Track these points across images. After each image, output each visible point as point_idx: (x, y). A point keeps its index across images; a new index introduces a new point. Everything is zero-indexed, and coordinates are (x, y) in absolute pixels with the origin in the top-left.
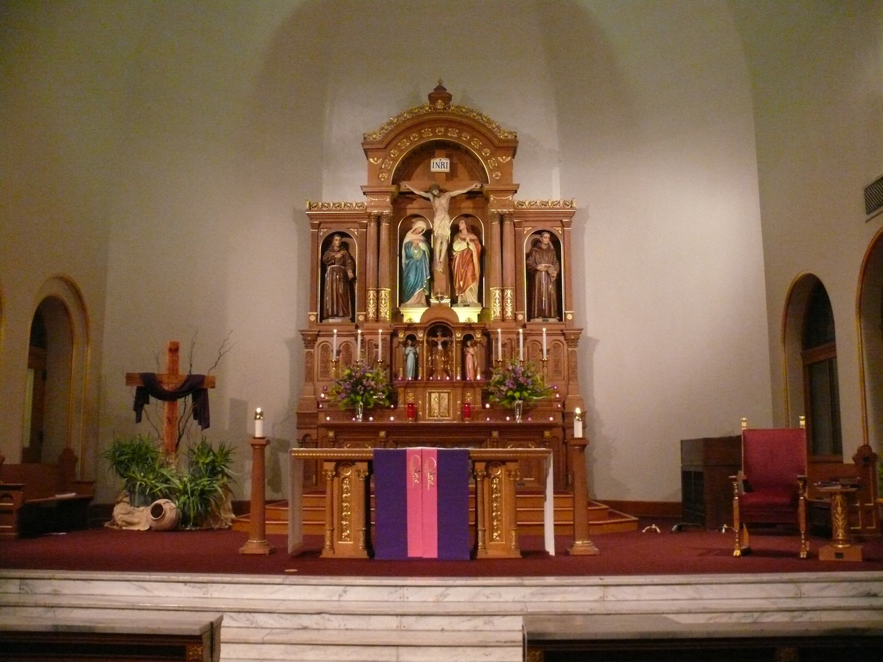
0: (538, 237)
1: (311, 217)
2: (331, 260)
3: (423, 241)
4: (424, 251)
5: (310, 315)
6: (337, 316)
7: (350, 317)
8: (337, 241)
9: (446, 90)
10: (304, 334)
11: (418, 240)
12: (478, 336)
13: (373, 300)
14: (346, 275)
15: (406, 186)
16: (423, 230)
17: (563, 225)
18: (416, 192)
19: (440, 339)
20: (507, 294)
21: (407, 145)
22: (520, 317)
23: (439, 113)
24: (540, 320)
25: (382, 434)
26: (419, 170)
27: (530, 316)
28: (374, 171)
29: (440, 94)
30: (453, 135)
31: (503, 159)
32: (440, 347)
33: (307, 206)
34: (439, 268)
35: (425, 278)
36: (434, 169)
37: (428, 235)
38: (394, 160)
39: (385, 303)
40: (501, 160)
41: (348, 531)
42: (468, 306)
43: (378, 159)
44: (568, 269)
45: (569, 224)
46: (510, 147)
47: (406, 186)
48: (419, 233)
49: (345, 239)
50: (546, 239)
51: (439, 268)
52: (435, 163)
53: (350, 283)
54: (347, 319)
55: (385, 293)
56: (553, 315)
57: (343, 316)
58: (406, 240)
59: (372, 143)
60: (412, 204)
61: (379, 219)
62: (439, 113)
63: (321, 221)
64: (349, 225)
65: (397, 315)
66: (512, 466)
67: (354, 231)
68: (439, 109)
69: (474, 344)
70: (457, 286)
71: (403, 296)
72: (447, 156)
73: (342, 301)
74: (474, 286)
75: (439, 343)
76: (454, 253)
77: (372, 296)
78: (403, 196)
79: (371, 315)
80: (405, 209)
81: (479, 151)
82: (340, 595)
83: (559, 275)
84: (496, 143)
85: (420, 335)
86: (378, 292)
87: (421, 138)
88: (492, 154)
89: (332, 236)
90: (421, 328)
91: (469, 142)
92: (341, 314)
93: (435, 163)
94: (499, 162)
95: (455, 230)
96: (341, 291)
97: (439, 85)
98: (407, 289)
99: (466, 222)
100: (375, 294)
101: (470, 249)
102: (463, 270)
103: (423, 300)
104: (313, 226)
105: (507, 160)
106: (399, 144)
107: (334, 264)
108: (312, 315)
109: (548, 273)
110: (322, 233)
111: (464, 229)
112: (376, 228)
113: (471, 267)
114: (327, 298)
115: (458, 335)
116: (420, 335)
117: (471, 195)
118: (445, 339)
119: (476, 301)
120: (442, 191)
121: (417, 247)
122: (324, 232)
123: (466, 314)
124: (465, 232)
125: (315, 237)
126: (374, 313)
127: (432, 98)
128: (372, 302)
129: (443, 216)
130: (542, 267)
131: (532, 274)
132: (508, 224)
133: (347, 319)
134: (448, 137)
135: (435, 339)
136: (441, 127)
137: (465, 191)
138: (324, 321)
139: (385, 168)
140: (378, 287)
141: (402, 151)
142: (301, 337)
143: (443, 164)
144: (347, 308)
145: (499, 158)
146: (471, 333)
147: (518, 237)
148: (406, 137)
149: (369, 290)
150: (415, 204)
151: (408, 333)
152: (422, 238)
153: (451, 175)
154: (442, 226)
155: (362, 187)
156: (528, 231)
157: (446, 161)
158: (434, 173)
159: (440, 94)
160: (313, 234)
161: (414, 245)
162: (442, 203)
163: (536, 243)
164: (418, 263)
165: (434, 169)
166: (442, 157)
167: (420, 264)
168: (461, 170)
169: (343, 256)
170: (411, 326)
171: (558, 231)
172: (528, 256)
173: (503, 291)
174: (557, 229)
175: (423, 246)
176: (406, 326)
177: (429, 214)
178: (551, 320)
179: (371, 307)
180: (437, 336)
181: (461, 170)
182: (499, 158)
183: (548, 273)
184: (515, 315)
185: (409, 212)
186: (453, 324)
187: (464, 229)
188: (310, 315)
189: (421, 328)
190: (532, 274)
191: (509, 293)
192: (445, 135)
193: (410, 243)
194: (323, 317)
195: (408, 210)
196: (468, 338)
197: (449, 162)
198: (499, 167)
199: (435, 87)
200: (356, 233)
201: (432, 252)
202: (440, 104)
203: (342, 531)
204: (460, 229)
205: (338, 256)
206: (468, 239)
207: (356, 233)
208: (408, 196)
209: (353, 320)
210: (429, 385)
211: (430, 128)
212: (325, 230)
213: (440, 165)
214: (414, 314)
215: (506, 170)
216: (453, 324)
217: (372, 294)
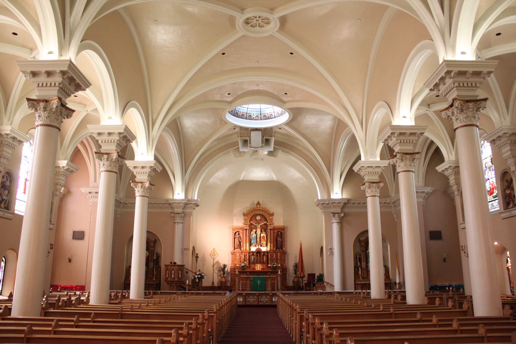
0: (278, 233)
1: (232, 228)
8: (237, 233)
10: (231, 253)
12: (266, 254)
14: (239, 241)
17: (283, 230)
18: (254, 224)
19: (259, 254)
21: (252, 215)
22: (274, 249)
24: (278, 250)
25: (248, 273)
27: (276, 249)
28: (245, 220)
29: (258, 203)
32: (259, 256)
34: (258, 240)
36: (257, 219)
37: (256, 232)
44: (284, 239)
45: (284, 230)
46: (272, 215)
47: (251, 222)
49: (239, 233)
50: (279, 233)
51: (258, 240)
53: (240, 242)
54: (240, 249)
55: (248, 244)
58: (251, 233)
59: (245, 214)
61: (246, 230)
65: (250, 249)
66: (271, 279)
67: (241, 231)
69: (265, 255)
70: (261, 243)
71: (250, 245)
72: (260, 216)
74: (265, 243)
79: (245, 249)
81: (266, 215)
84: (270, 214)
85: (255, 254)
86: (246, 244)
87: (255, 213)
88: (269, 217)
91: (264, 214)
95: (261, 231)
103: (255, 246)
104: (233, 230)
109: (280, 241)
114: (236, 245)
115: (262, 254)
116: (255, 254)
117: (265, 224)
119: (265, 246)
121: (254, 235)
122: (235, 231)
123: (264, 249)
124: (263, 232)
125: (233, 232)
127: (257, 205)
130: (279, 239)
131: (277, 240)
132: (272, 230)
137: (263, 224)
147: (274, 233)
148: (252, 213)
150: (253, 226)
153: (260, 220)
154: (259, 232)
156: (276, 231)
157: (260, 217)
159: (258, 203)
162: (259, 226)
163: (278, 234)
165: (257, 219)
169: (239, 237)
170: (253, 252)
171: (282, 231)
172: (276, 236)
173: (271, 244)
175: (255, 235)
177: (256, 228)
183: (280, 241)
184: (273, 249)
185: (252, 227)
190: (277, 240)
191: (272, 245)
193: (252, 234)
194: (234, 249)
196: (264, 254)
198: (270, 219)
201: (257, 235)
202: (258, 206)
205: (238, 236)
206: (264, 233)
209: (241, 250)
210: (257, 263)
213: (258, 218)
214: (253, 249)
215: (271, 220)
217: (245, 245)
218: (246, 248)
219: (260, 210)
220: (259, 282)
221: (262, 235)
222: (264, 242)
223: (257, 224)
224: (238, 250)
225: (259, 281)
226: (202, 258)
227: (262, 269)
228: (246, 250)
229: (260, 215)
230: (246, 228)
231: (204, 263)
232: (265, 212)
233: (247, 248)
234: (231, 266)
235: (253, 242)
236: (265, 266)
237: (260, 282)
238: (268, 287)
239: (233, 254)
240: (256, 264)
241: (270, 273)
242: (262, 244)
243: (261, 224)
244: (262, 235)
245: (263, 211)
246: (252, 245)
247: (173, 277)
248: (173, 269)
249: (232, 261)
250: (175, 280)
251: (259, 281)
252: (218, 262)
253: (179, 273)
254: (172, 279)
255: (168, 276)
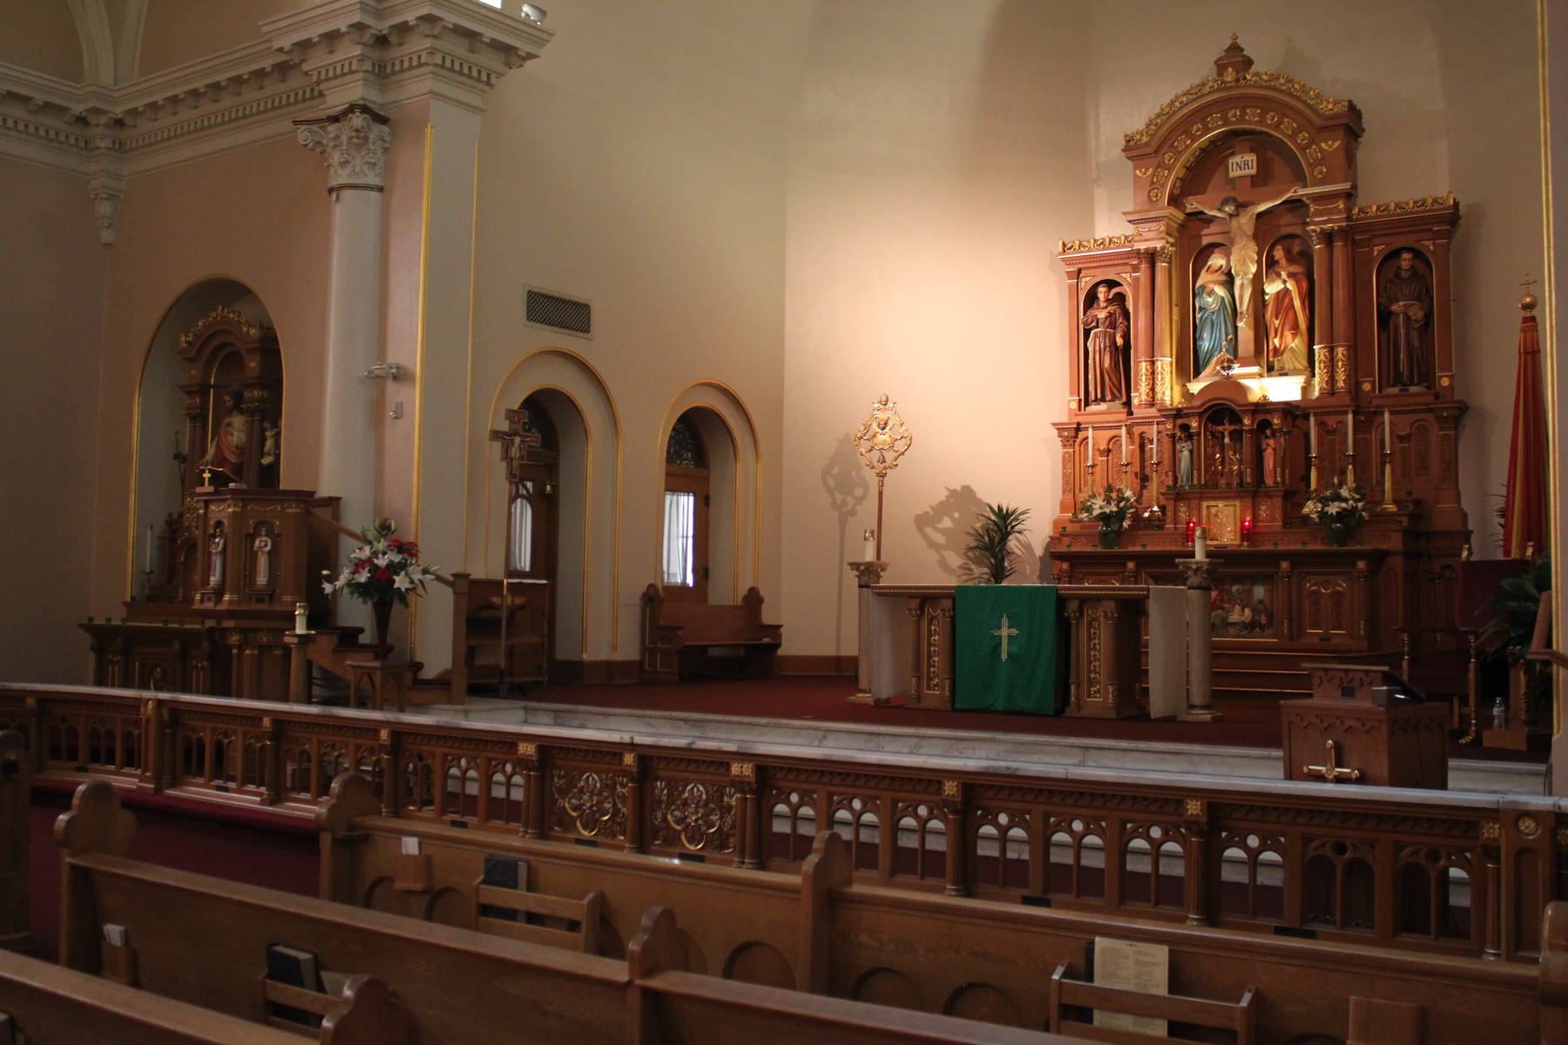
1: (1068, 262)
2: (1092, 322)
3: (1222, 284)
4: (1223, 298)
5: (1070, 401)
6: (1103, 399)
7: (1124, 399)
9: (1242, 50)
10: (1060, 428)
11: (1210, 282)
13: (1146, 375)
15: (1193, 205)
16: (1221, 266)
20: (1337, 354)
22: (1367, 387)
23: (1230, 88)
24: (1394, 390)
26: (1217, 178)
29: (1236, 58)
30: (1252, 119)
31: (1327, 145)
33: (1060, 249)
35: (1224, 338)
36: (1234, 173)
38: (1170, 169)
39: (1162, 379)
40: (1326, 148)
41: (937, 680)
42: (1286, 374)
43: (1147, 170)
47: (1193, 205)
48: (1217, 271)
52: (1235, 166)
54: (1117, 405)
56: (1416, 380)
57: (1111, 401)
59: (1137, 148)
60: (1208, 227)
61: (1151, 257)
62: (1230, 88)
63: (1080, 266)
64: (1119, 269)
67: (1126, 277)
68: (1230, 82)
72: (1252, 151)
73: (1110, 379)
75: (1226, 433)
76: (1267, 297)
77: (1144, 370)
78: (1194, 218)
80: (1200, 237)
82: (820, 741)
83: (1428, 316)
86: (1153, 363)
88: (1312, 142)
89: (1097, 285)
90: (1193, 414)
91: (1277, 126)
92: (1109, 397)
93: (1235, 166)
94: (1321, 150)
96: (1107, 364)
97: (1232, 44)
98: (1201, 356)
99: (1283, 249)
100: (1149, 367)
101: (1288, 289)
102: (1277, 322)
104: (1070, 275)
105: (1335, 147)
106: (1176, 144)
107: (1097, 327)
108: (1073, 400)
109: (1408, 318)
110: (1083, 284)
111: (1281, 259)
112: (1148, 271)
113: (1291, 315)
116: (1194, 424)
118: (1232, 428)
120: (1241, 206)
122: (1086, 282)
126: (1147, 394)
127: (1221, 67)
128: (1144, 378)
129: (1244, 243)
132: (1338, 244)
133: (1117, 405)
134: (1246, 122)
135: (1220, 428)
136: (1236, 108)
138: (1089, 409)
139: (1158, 181)
140: (1153, 356)
141: (1180, 152)
142: (1056, 432)
143: (1246, 163)
144: (1120, 391)
145: (1323, 145)
146: (1268, 417)
148: (1185, 132)
149: (1141, 362)
150: (1214, 228)
151: (1179, 422)
152: (1224, 278)
155: (1125, 214)
157: (1251, 158)
158: (1234, 179)
159: (1236, 58)
160: (1070, 285)
161: (1207, 290)
162: (1246, 221)
164: (1214, 317)
165: (1234, 173)
166: (1243, 152)
167: (1217, 318)
168: (1279, 167)
169: (1110, 315)
173: (1331, 350)
174: (1426, 243)
175: (1220, 291)
176: (1174, 412)
178: (1413, 389)
179: (1144, 385)
180: (1224, 425)
181: (1279, 167)
182: (1323, 145)
183: (1408, 318)
185: (1205, 241)
186: (1238, 406)
187: (1281, 259)
188: (1070, 401)
189: (1193, 414)
191: (1340, 352)
192: (1242, 119)
193: (1203, 287)
195: (1203, 238)
197: (1254, 158)
199: (1226, 47)
200: (1129, 279)
202: (1230, 75)
203: (930, 679)
204: (1276, 258)
207: (1129, 279)
208: (1199, 218)
211: (1218, 112)
212: (1088, 279)
213: (1242, 164)
216: (1238, 406)
218: (1153, 389)
219: (1244, 101)
220: (1005, 632)
221: (1272, 288)
222: (1288, 335)
223: (1229, 209)
224: (1103, 407)
225: (1005, 621)
226: (836, 471)
227: (1247, 534)
228: (1152, 404)
229: (1257, 141)
230: (1142, 246)
231: (850, 501)
232: (1283, 109)
233: (1158, 388)
234: (1056, 523)
235: (1205, 345)
236: (1273, 519)
237: (1014, 631)
238: (1091, 683)
239: (1072, 434)
240: (1202, 499)
241: (1292, 565)
242: (1277, 352)
243: (1262, 208)
244: (1272, 288)
245: (1265, 104)
246: (1205, 366)
247: (262, 579)
248: (258, 526)
249: (1071, 484)
250: (277, 608)
251: (1005, 621)
252: (964, 496)
253: (253, 556)
254: (260, 600)
255: (272, 576)
